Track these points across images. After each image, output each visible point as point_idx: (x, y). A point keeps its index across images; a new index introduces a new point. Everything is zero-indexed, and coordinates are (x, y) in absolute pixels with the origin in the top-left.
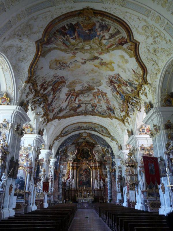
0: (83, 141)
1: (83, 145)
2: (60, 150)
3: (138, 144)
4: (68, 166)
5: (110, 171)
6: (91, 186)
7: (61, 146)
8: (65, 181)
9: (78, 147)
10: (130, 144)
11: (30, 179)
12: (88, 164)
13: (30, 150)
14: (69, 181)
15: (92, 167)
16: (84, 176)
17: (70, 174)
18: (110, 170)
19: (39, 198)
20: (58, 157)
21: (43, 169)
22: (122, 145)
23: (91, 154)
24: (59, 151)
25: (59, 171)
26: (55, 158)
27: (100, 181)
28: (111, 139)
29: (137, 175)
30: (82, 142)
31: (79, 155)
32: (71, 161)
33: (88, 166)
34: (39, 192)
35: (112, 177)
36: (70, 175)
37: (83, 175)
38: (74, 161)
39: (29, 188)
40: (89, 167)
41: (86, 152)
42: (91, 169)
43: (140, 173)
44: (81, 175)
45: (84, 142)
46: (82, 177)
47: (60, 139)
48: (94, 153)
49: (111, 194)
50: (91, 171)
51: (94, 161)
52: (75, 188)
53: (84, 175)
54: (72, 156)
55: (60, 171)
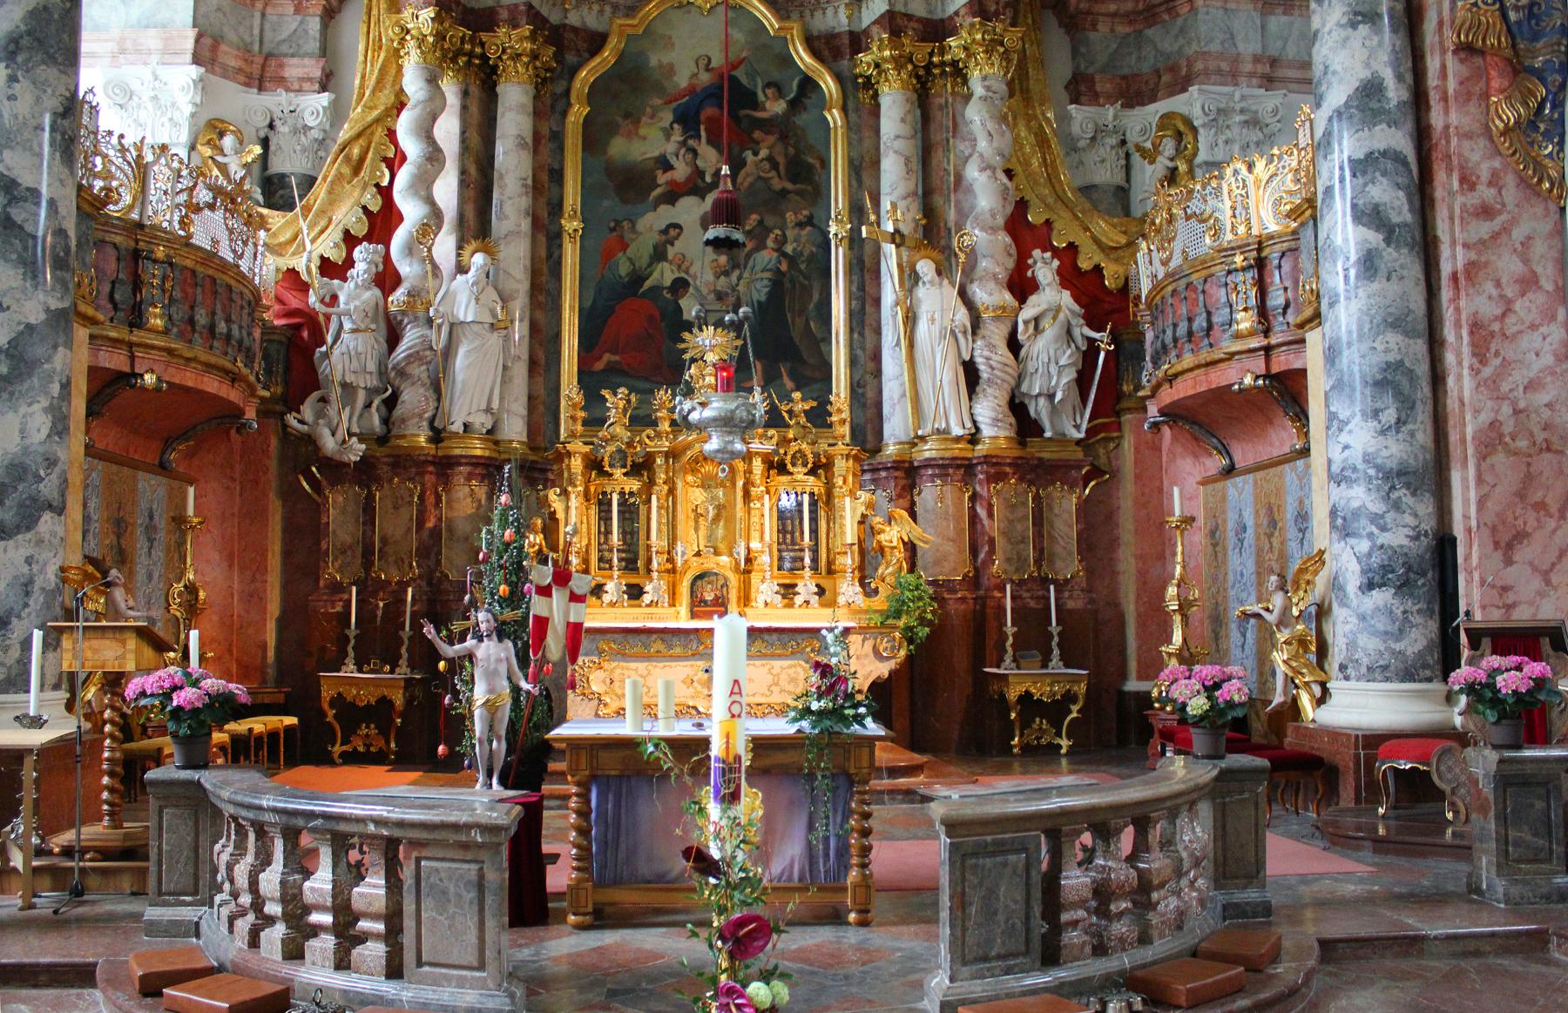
14: (387, 279)
15: (858, 41)
16: (690, 210)
27: (1022, 286)
37: (671, 197)
42: (828, 84)
52: (515, 430)
53: (696, 186)
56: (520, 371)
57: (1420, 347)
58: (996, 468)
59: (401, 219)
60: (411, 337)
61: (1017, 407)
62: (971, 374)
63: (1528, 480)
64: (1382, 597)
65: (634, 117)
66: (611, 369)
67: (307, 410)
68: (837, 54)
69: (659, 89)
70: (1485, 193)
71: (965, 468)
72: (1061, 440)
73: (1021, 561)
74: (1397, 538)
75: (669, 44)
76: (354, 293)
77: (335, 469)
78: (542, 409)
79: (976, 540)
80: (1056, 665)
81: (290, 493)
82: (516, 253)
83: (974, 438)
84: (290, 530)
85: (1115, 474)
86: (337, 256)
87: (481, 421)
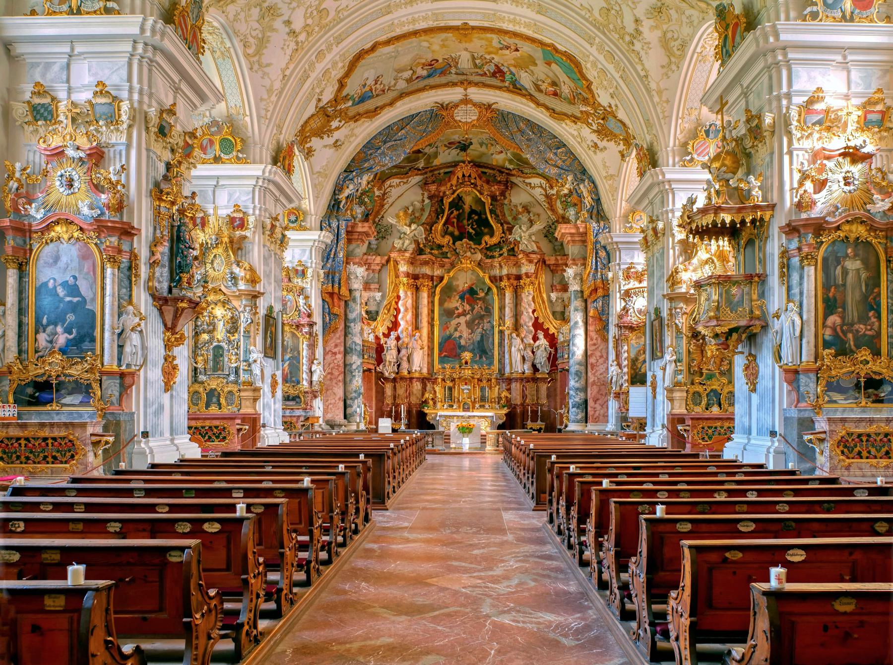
0: (457, 159)
1: (460, 176)
2: (347, 192)
3: (790, 84)
4: (393, 273)
5: (582, 292)
6: (491, 364)
7: (351, 170)
8: (377, 338)
9: (433, 188)
10: (731, 99)
11: (125, 300)
12: (479, 265)
13: (113, 119)
14: (398, 339)
15: (501, 279)
16: (462, 320)
17: (402, 309)
18: (585, 288)
19: (236, 409)
20: (334, 224)
21: (246, 265)
22: (656, 148)
23: (498, 221)
24: (343, 196)
25: (344, 291)
26: (321, 229)
27: (535, 339)
28: (598, 132)
29: (762, 279)
30: (455, 164)
31: (440, 226)
32: (402, 251)
33: (481, 274)
34: (232, 382)
35: (590, 320)
36: (398, 311)
37: (459, 316)
38: (420, 251)
39: (121, 347)
40: (487, 281)
41: (473, 212)
42: (495, 290)
43: (782, 266)
44: (449, 314)
45: (464, 162)
46: (456, 321)
47: (338, 128)
48: (509, 219)
49: (582, 395)
50: (496, 298)
51: (509, 251)
52: (425, 371)
53: (464, 314)
54: (407, 230)
55: (350, 291)
56: (426, 357)
57: (583, 368)
58: (528, 380)
59: (400, 325)
60: (403, 352)
61: (534, 366)
62: (523, 358)
63: (600, 390)
64: (575, 409)
65: (450, 297)
66: (445, 356)
67: (381, 367)
68: (496, 281)
69: (455, 291)
70: (595, 341)
71: (522, 379)
72: (543, 373)
73: (533, 400)
74: (577, 400)
75: (458, 280)
76: (391, 342)
77: (386, 379)
78: (431, 365)
79: (524, 397)
80: (539, 422)
81: (377, 384)
82: (425, 331)
83: (524, 373)
84: (377, 392)
85: (556, 380)
86: (386, 332)
87: (418, 369)
